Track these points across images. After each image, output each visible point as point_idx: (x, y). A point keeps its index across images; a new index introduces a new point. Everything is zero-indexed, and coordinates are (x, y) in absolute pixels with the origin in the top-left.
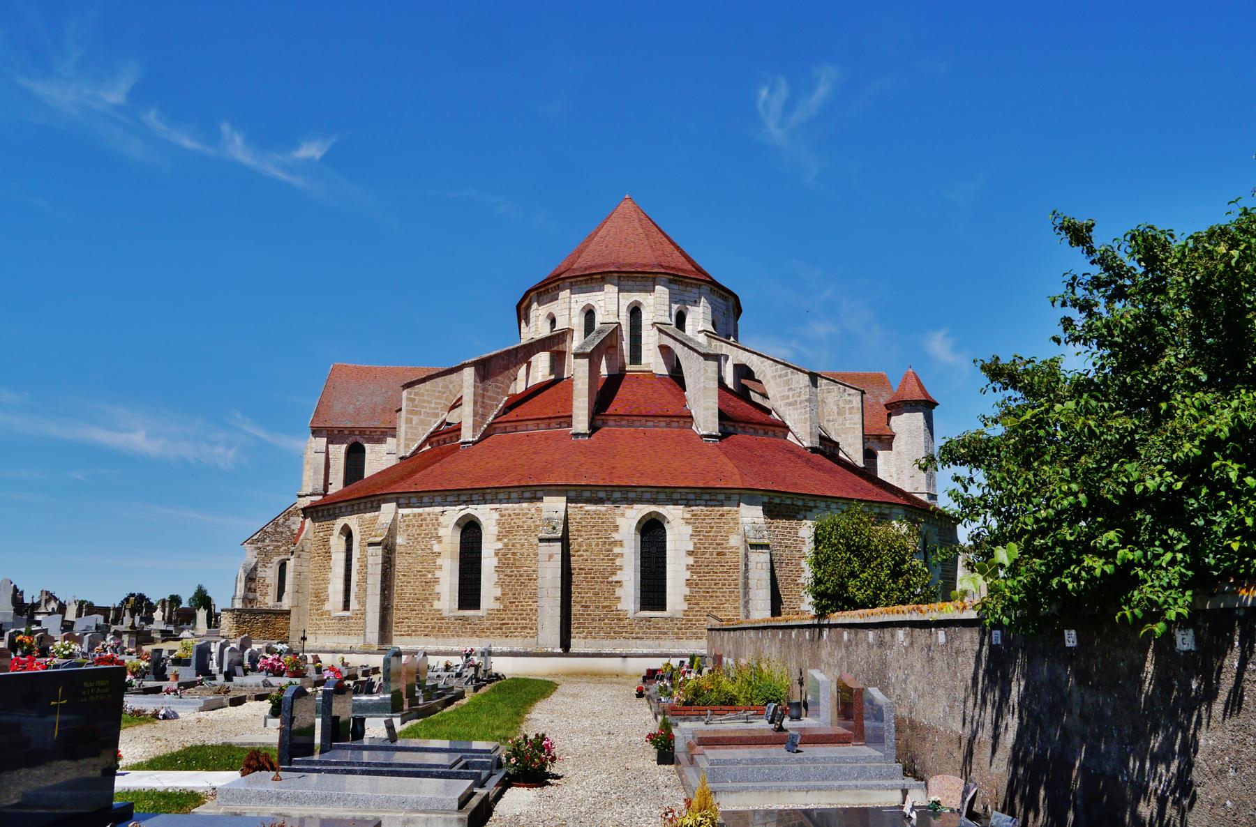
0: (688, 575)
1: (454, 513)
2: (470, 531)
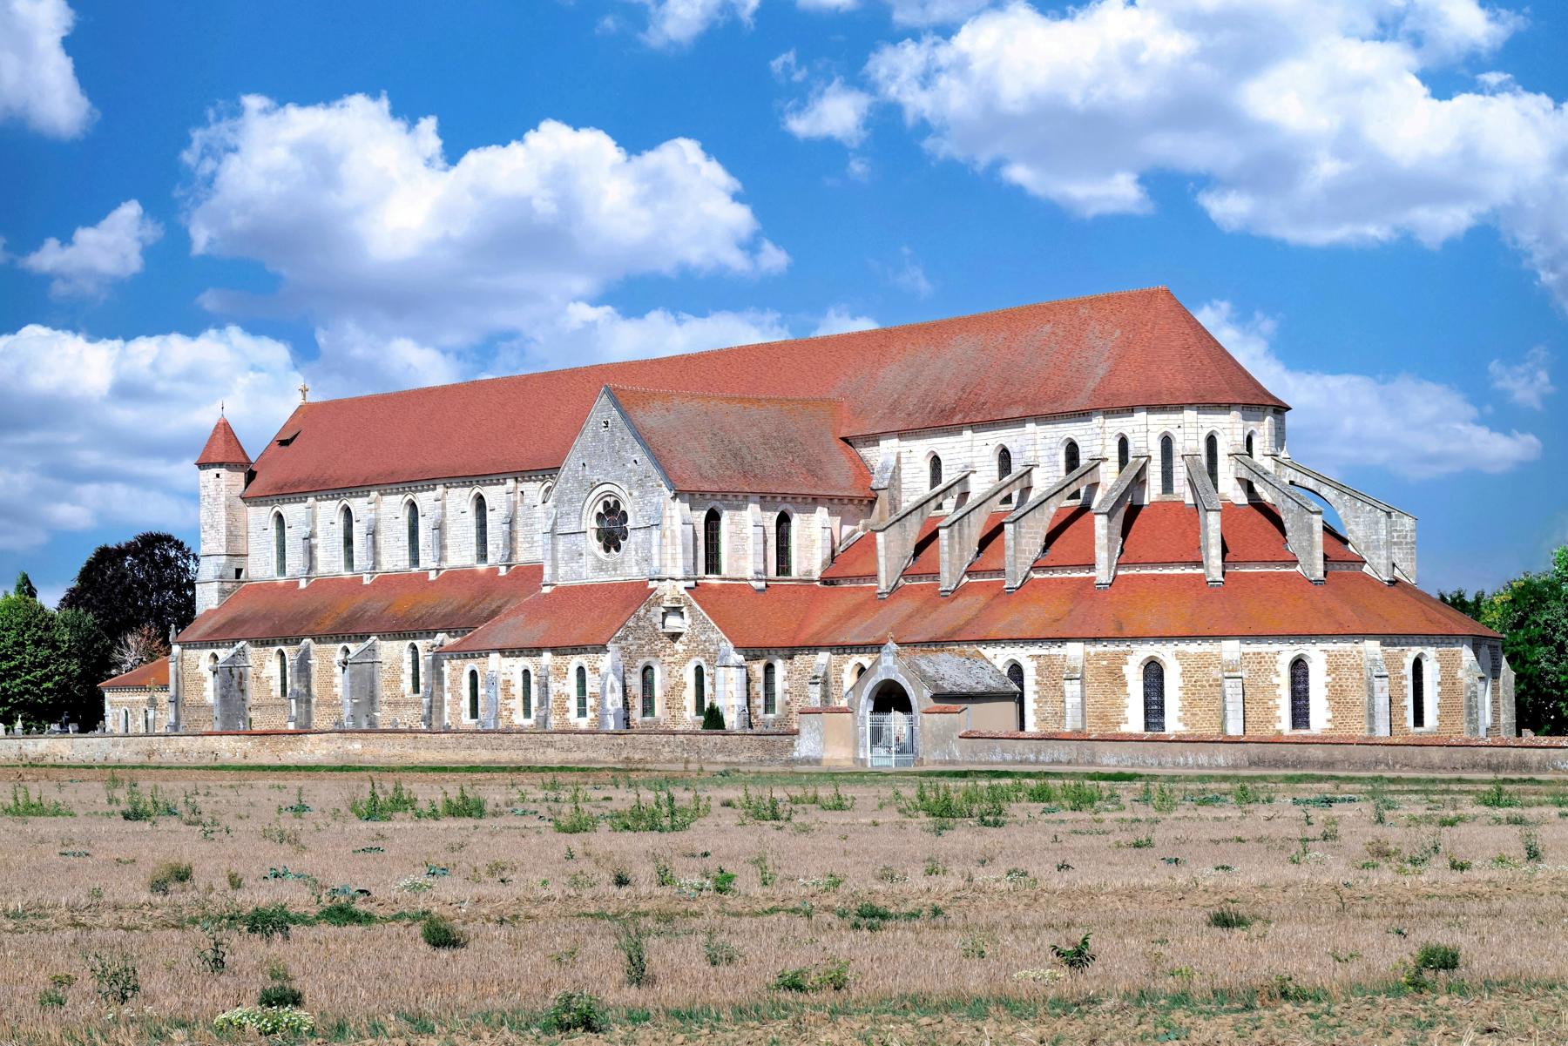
0: (1438, 700)
1: (1286, 653)
2: (1299, 667)
